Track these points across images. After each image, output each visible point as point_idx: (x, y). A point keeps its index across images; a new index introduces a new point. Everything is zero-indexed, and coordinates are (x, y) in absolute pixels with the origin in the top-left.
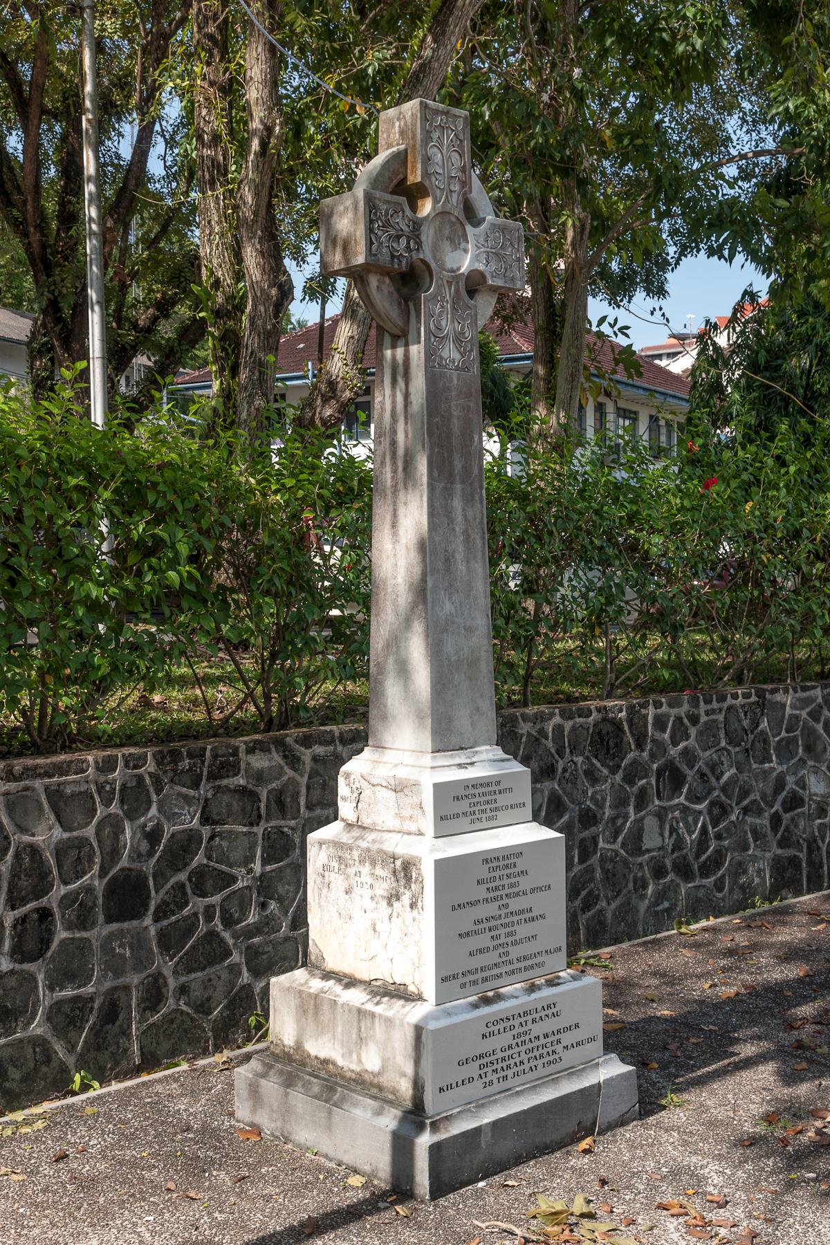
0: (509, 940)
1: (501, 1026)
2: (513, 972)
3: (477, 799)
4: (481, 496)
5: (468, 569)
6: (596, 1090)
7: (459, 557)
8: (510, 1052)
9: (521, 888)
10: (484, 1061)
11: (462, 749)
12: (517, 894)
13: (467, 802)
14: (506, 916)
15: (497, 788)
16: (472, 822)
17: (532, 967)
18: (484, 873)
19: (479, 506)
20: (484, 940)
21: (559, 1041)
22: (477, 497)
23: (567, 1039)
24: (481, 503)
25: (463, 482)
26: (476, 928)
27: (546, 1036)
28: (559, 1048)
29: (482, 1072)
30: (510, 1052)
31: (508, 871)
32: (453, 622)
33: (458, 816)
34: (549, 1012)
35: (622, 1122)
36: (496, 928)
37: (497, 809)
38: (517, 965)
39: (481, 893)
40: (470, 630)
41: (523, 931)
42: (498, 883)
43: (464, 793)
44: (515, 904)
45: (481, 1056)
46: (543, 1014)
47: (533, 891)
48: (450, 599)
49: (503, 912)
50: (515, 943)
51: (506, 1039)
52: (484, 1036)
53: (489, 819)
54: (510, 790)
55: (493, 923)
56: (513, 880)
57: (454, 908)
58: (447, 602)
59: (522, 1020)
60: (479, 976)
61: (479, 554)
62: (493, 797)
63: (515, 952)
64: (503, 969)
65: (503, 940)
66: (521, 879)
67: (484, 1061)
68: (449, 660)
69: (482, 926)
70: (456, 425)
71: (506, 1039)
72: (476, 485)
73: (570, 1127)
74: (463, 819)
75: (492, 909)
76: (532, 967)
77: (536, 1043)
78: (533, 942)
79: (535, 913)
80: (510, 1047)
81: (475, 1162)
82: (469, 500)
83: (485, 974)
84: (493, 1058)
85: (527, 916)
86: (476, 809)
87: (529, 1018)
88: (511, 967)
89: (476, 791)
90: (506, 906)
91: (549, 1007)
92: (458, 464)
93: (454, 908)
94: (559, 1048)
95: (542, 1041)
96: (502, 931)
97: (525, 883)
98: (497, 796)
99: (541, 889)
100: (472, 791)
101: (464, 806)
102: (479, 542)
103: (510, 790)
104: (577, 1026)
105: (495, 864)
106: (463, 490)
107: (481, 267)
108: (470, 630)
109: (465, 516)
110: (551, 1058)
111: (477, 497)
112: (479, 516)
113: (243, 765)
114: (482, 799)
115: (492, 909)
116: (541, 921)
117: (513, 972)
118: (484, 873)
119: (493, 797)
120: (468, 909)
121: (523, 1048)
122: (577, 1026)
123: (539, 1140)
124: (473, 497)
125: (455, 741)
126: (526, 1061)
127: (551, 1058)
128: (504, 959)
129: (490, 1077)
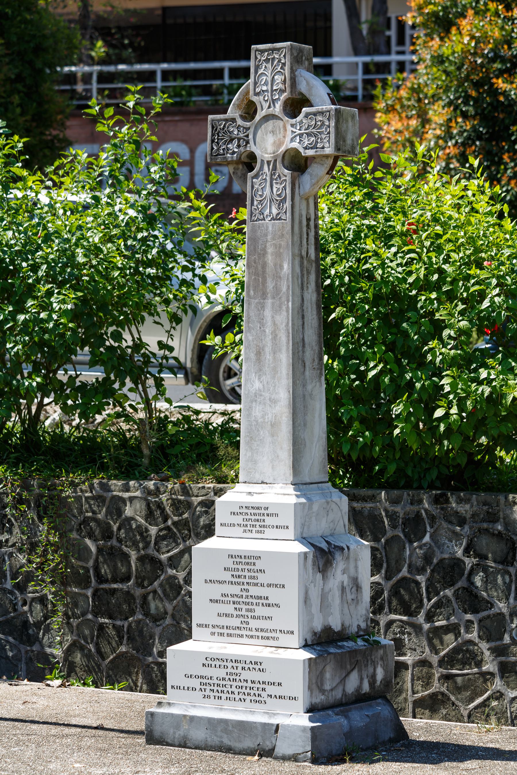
0: (250, 614)
1: (218, 663)
2: (252, 637)
3: (249, 517)
4: (288, 308)
5: (274, 358)
6: (274, 728)
7: (268, 349)
8: (224, 683)
9: (259, 581)
10: (205, 681)
11: (263, 483)
12: (256, 585)
13: (241, 517)
14: (247, 597)
15: (266, 512)
16: (245, 531)
17: (268, 638)
18: (229, 563)
19: (284, 313)
20: (230, 609)
21: (264, 690)
22: (284, 308)
23: (271, 690)
24: (287, 311)
25: (274, 298)
26: (222, 598)
27: (253, 682)
28: (264, 694)
29: (202, 687)
30: (224, 683)
31: (249, 567)
32: (261, 395)
33: (234, 525)
34: (257, 667)
35: (295, 758)
36: (239, 603)
37: (264, 526)
38: (254, 633)
39: (227, 576)
40: (274, 402)
41: (260, 611)
42: (240, 573)
43: (239, 511)
44: (254, 591)
45: (202, 677)
46: (251, 666)
47: (269, 585)
48: (259, 379)
49: (244, 594)
50: (254, 617)
51: (222, 673)
52: (204, 665)
53: (258, 532)
54: (277, 515)
55: (236, 599)
56: (253, 574)
57: (206, 582)
58: (257, 381)
59: (235, 665)
60: (225, 631)
61: (284, 349)
62: (262, 518)
63: (254, 624)
64: (244, 632)
65: (244, 613)
66: (259, 575)
67: (205, 681)
68: (257, 421)
69: (226, 599)
70: (270, 259)
71: (222, 673)
72: (284, 299)
73: (248, 743)
74: (237, 528)
75: (236, 590)
76: (268, 638)
77: (245, 684)
78: (268, 621)
79: (270, 601)
80: (224, 679)
81: (177, 736)
82: (277, 309)
83: (229, 631)
84: (209, 681)
85: (265, 602)
86: (248, 523)
87: (240, 666)
88: (250, 633)
89: (249, 511)
90: (247, 591)
91: (256, 663)
92: (270, 285)
93: (206, 582)
94: (264, 694)
95: (249, 684)
96: (244, 607)
97: (262, 578)
98: (266, 518)
99: (276, 586)
100: (244, 510)
101: (239, 519)
102: (284, 339)
103: (277, 515)
104: (280, 684)
105: (238, 560)
106: (273, 304)
107: (295, 145)
108: (274, 402)
109: (275, 324)
110: (258, 699)
111: (284, 308)
112: (285, 321)
113: (501, 515)
114: (253, 517)
115: (236, 590)
116: (275, 608)
117: (252, 637)
118: (229, 563)
119: (262, 518)
120: (217, 585)
121: (234, 684)
122: (280, 684)
123: (227, 741)
124: (280, 307)
125: (258, 477)
126: (236, 693)
127: (258, 699)
128: (245, 626)
129: (208, 693)
